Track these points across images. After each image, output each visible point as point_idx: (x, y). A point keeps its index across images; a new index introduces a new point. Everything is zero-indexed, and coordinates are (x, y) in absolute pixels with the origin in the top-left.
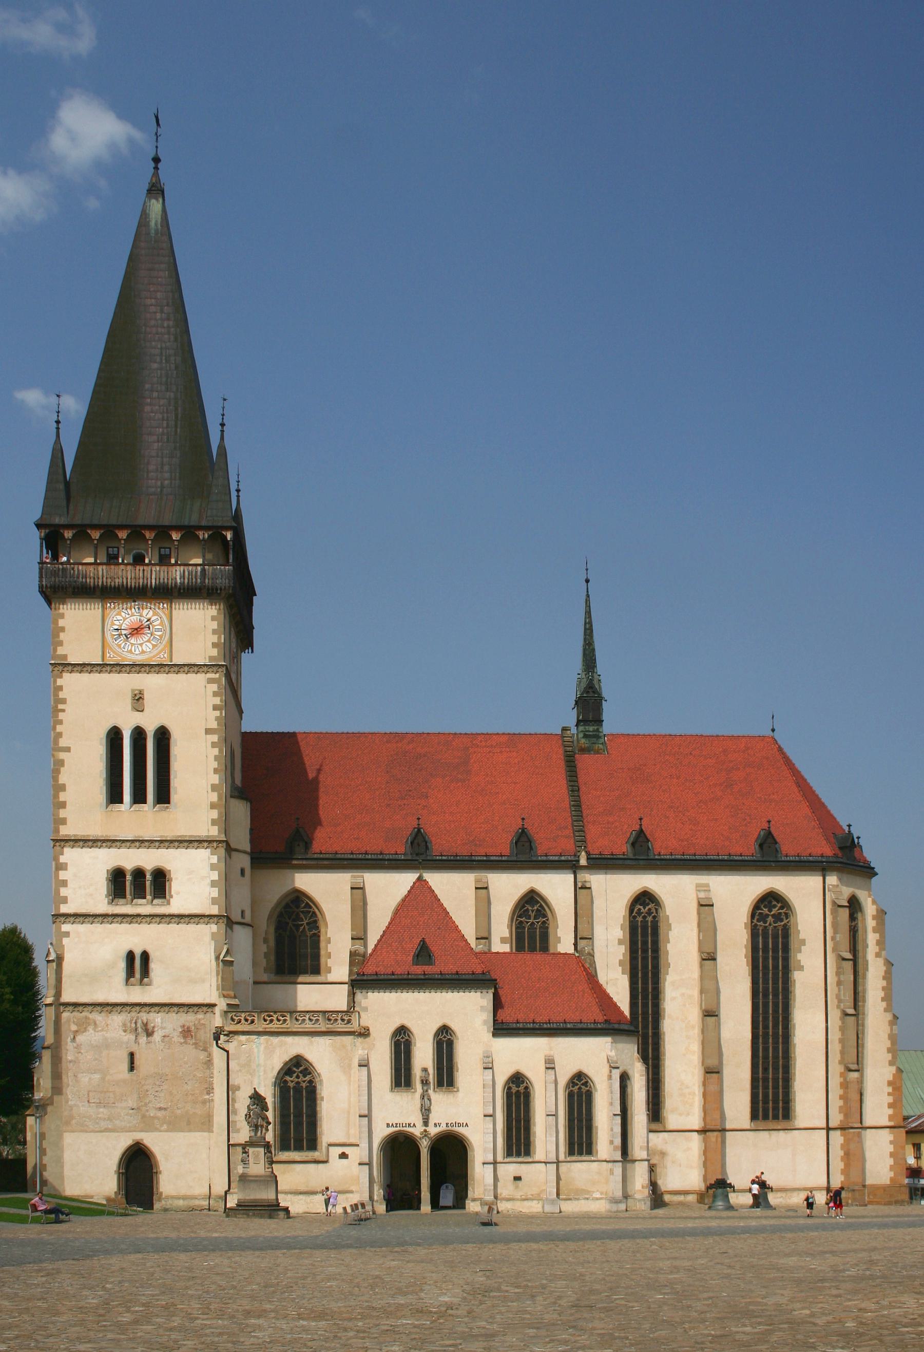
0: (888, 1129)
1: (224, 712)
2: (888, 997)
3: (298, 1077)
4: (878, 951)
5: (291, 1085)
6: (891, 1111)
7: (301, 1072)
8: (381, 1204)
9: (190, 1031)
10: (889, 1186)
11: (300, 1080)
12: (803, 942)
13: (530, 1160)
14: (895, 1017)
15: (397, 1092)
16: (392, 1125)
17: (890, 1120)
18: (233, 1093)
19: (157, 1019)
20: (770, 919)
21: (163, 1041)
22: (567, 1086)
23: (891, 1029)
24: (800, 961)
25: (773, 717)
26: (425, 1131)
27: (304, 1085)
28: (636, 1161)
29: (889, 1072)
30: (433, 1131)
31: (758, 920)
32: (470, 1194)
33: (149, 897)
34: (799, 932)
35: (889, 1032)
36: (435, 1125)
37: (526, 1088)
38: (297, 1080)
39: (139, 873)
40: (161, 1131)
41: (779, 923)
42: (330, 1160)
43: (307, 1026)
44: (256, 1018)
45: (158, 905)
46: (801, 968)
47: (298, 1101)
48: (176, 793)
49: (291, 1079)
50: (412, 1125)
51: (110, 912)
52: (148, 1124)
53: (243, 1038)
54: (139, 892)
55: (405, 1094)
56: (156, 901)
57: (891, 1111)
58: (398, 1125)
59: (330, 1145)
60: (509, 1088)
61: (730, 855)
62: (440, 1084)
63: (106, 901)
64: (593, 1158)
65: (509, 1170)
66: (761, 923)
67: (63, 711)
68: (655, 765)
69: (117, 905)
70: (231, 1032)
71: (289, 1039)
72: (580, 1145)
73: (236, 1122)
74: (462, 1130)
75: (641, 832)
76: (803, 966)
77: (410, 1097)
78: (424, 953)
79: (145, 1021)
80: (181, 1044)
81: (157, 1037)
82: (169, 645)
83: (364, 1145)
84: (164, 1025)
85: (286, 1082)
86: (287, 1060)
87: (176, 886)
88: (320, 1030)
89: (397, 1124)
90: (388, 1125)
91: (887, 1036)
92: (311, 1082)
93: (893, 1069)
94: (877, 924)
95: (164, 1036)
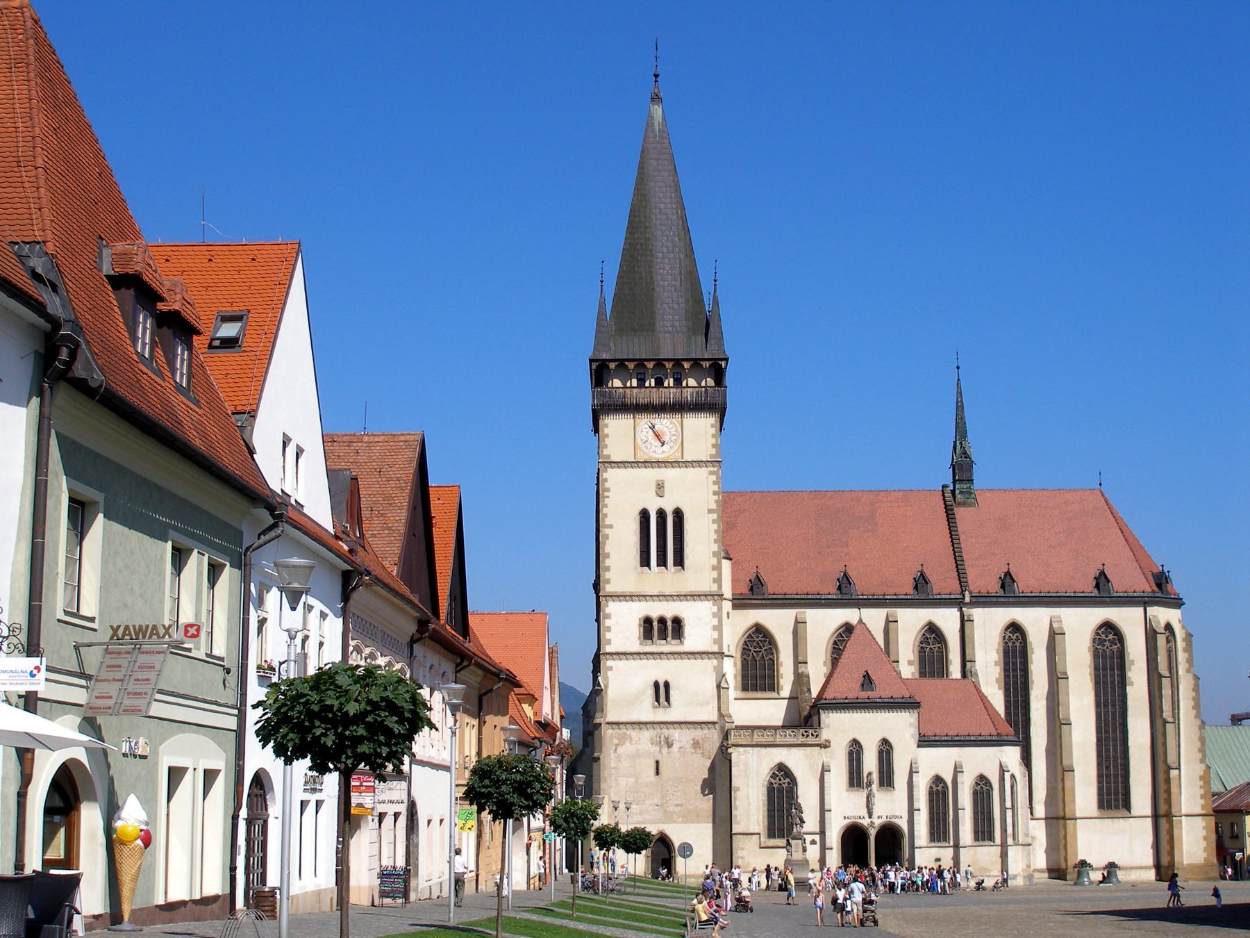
0: (1201, 817)
1: (720, 496)
2: (1197, 706)
3: (780, 780)
4: (1187, 667)
5: (776, 786)
6: (1202, 802)
9: (698, 743)
10: (1204, 865)
12: (1132, 663)
13: (947, 845)
14: (1203, 722)
15: (852, 791)
17: (1202, 809)
18: (734, 793)
19: (675, 734)
20: (1107, 644)
21: (679, 751)
23: (1201, 733)
24: (1130, 678)
25: (1100, 474)
26: (871, 822)
27: (784, 786)
29: (1200, 769)
30: (878, 822)
31: (1098, 646)
33: (669, 639)
34: (1129, 654)
35: (1199, 735)
36: (879, 817)
39: (662, 621)
41: (1114, 647)
43: (788, 740)
46: (1132, 684)
47: (780, 798)
48: (687, 559)
52: (668, 818)
53: (741, 749)
54: (663, 635)
55: (856, 793)
56: (674, 642)
57: (1202, 802)
60: (931, 787)
62: (881, 784)
63: (639, 642)
66: (1100, 647)
68: (1014, 516)
69: (646, 645)
70: (733, 745)
71: (774, 750)
72: (983, 833)
73: (736, 816)
74: (897, 821)
75: (1008, 574)
76: (1133, 682)
78: (867, 681)
79: (666, 736)
80: (692, 753)
81: (675, 748)
82: (680, 450)
84: (680, 739)
85: (771, 783)
87: (688, 630)
88: (796, 743)
91: (1197, 739)
93: (1203, 766)
94: (1187, 645)
95: (680, 748)
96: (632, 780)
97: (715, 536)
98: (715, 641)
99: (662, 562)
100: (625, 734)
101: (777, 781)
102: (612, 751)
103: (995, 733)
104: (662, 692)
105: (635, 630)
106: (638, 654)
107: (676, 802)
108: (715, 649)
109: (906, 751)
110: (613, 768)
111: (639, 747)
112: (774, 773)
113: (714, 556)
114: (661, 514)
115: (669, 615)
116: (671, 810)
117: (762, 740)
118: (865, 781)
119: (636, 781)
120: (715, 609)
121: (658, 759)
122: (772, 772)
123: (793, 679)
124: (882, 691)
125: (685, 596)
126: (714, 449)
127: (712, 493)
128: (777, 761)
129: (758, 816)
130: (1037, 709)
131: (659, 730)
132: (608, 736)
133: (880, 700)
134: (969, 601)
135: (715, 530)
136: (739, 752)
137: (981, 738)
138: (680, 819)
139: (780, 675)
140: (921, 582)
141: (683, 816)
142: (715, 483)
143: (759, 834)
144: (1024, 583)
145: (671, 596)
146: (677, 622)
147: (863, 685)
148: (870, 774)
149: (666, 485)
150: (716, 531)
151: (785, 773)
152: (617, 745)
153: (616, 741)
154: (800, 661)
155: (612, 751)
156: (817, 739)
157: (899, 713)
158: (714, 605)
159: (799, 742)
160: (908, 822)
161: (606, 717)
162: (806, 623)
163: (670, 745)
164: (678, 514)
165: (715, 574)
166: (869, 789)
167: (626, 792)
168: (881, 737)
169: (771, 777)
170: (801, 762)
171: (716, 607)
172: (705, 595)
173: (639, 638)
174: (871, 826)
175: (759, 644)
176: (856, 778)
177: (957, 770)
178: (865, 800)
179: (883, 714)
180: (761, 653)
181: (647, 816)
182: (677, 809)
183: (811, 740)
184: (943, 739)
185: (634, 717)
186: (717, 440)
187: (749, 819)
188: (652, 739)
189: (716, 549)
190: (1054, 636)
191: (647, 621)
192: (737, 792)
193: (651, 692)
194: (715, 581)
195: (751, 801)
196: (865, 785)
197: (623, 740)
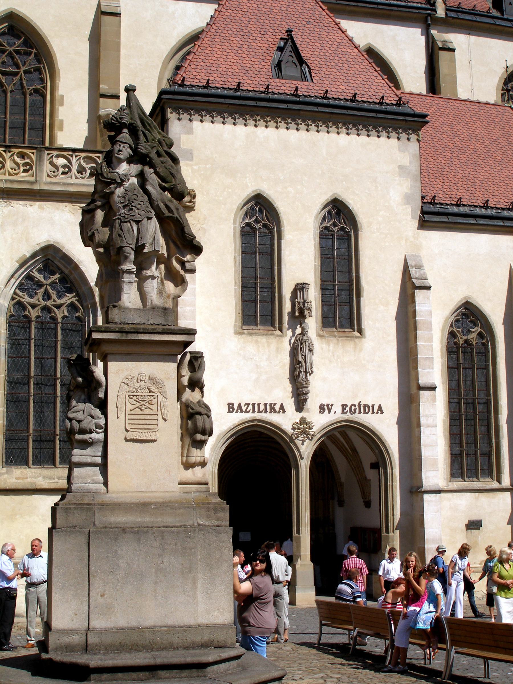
3: (47, 296)
5: (34, 313)
7: (53, 285)
11: (49, 303)
13: (495, 485)
15: (250, 334)
16: (240, 405)
26: (303, 421)
27: (59, 314)
38: (43, 303)
43: (74, 181)
49: (32, 301)
50: (277, 408)
55: (263, 340)
58: (251, 407)
77: (273, 346)
89: (248, 404)
90: (231, 407)
101: (38, 298)
112: (29, 277)
118: (287, 307)
122: (22, 273)
123: (86, 134)
134: (444, 16)
139: (57, 124)
147: (279, 65)
151: (63, 280)
154: (102, 91)
157: (373, 139)
160: (399, 422)
162: (118, 15)
166: (299, 330)
169: (21, 287)
174: (304, 432)
175: (13, 58)
178: (286, 360)
179: (333, 136)
180: (18, 77)
184: (478, 211)
196: (286, 319)
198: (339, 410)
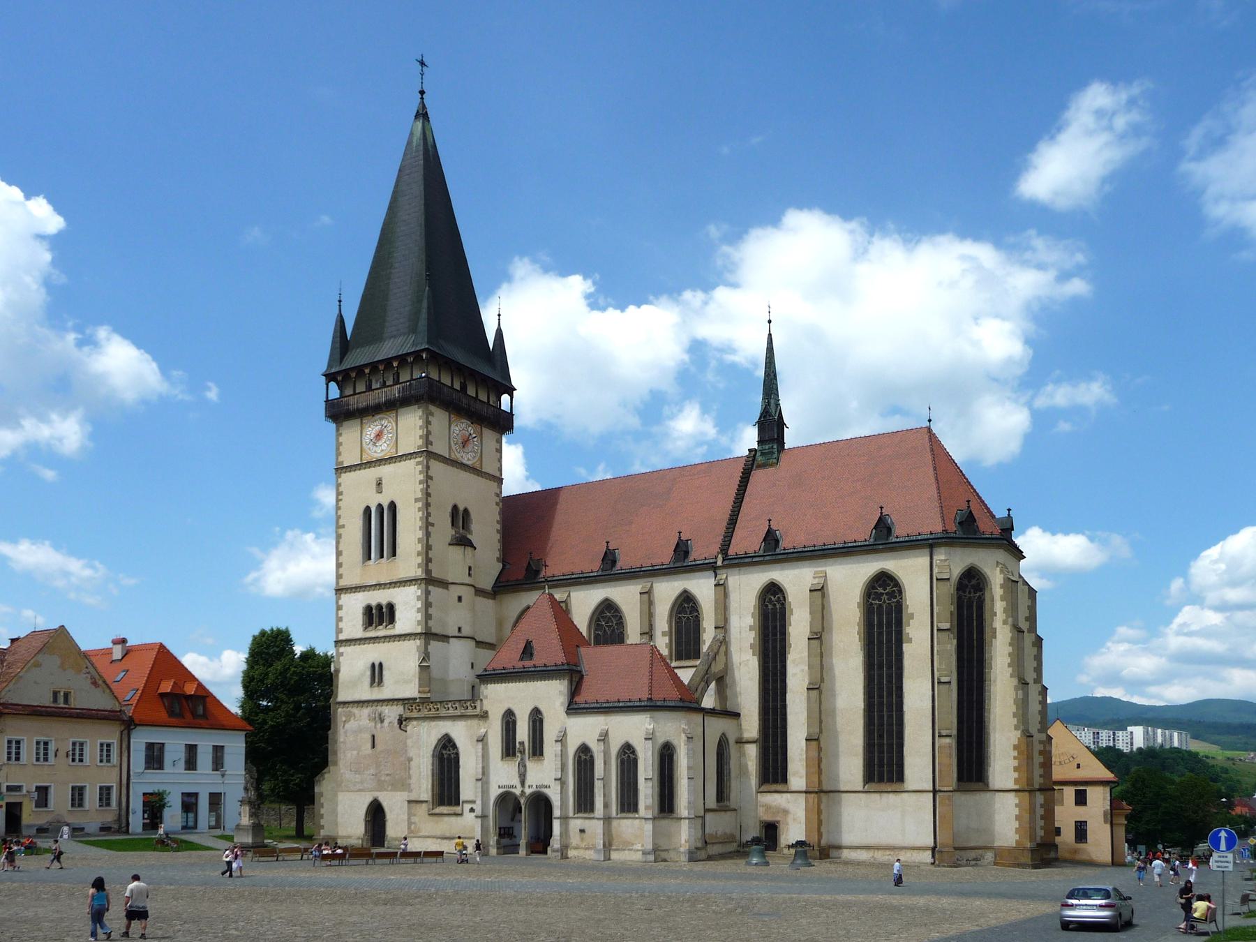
3: (449, 750)
5: (445, 756)
8: (494, 848)
13: (592, 816)
22: (619, 755)
27: (452, 756)
28: (681, 818)
30: (528, 791)
32: (551, 844)
33: (384, 624)
36: (529, 787)
37: (592, 757)
39: (380, 607)
40: (387, 791)
42: (465, 814)
44: (421, 707)
45: (389, 629)
51: (363, 637)
53: (415, 723)
55: (510, 762)
59: (463, 802)
60: (580, 757)
61: (845, 543)
64: (637, 816)
65: (576, 824)
67: (341, 500)
71: (441, 723)
72: (629, 804)
74: (546, 791)
81: (386, 723)
82: (395, 448)
83: (479, 802)
86: (440, 737)
87: (398, 615)
92: (457, 754)
95: (390, 723)
96: (355, 753)
97: (419, 524)
98: (419, 623)
99: (382, 556)
100: (350, 712)
102: (341, 727)
103: (645, 696)
104: (377, 673)
105: (359, 618)
106: (360, 640)
107: (388, 772)
108: (419, 630)
109: (556, 719)
110: (342, 742)
111: (361, 723)
113: (419, 543)
114: (380, 506)
115: (384, 602)
116: (383, 779)
117: (451, 712)
119: (358, 754)
120: (419, 592)
121: (373, 733)
124: (539, 660)
125: (395, 583)
126: (421, 440)
127: (418, 481)
128: (443, 732)
129: (427, 785)
130: (743, 669)
131: (374, 707)
132: (339, 714)
133: (533, 669)
135: (420, 517)
136: (413, 725)
137: (631, 704)
138: (390, 788)
140: (682, 549)
141: (392, 784)
142: (421, 472)
143: (427, 802)
144: (786, 543)
145: (385, 584)
146: (391, 607)
148: (522, 743)
149: (384, 482)
150: (421, 519)
152: (345, 721)
153: (344, 719)
155: (341, 727)
156: (475, 710)
158: (418, 589)
159: (459, 714)
161: (337, 697)
163: (382, 721)
164: (393, 506)
165: (419, 560)
167: (351, 763)
168: (533, 707)
170: (461, 732)
171: (420, 591)
172: (411, 581)
173: (363, 625)
176: (510, 749)
177: (604, 737)
181: (365, 785)
182: (387, 778)
183: (470, 712)
185: (357, 697)
186: (423, 431)
187: (420, 787)
188: (369, 716)
189: (421, 536)
190: (819, 591)
191: (368, 610)
192: (411, 763)
193: (368, 673)
194: (419, 566)
195: (422, 770)
197: (350, 716)
198: (534, 787)
